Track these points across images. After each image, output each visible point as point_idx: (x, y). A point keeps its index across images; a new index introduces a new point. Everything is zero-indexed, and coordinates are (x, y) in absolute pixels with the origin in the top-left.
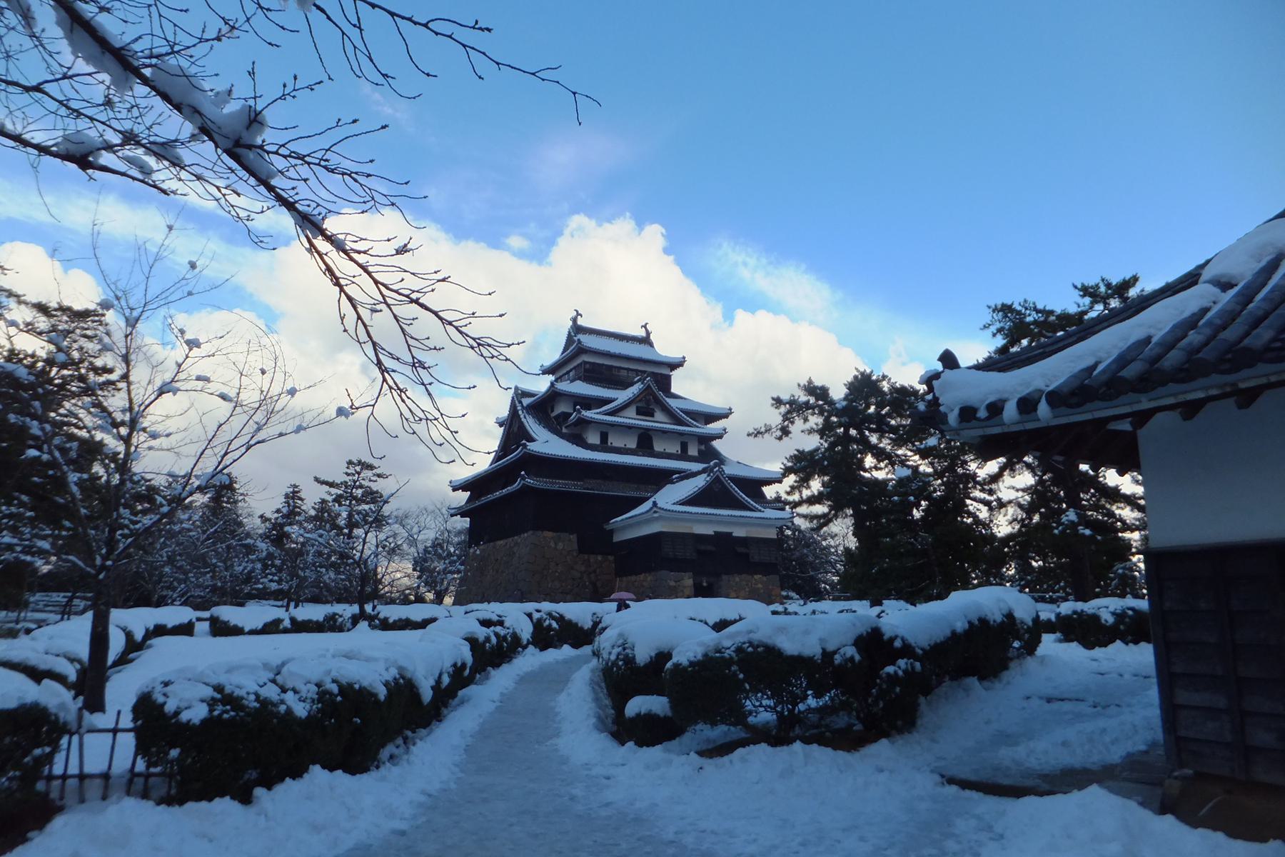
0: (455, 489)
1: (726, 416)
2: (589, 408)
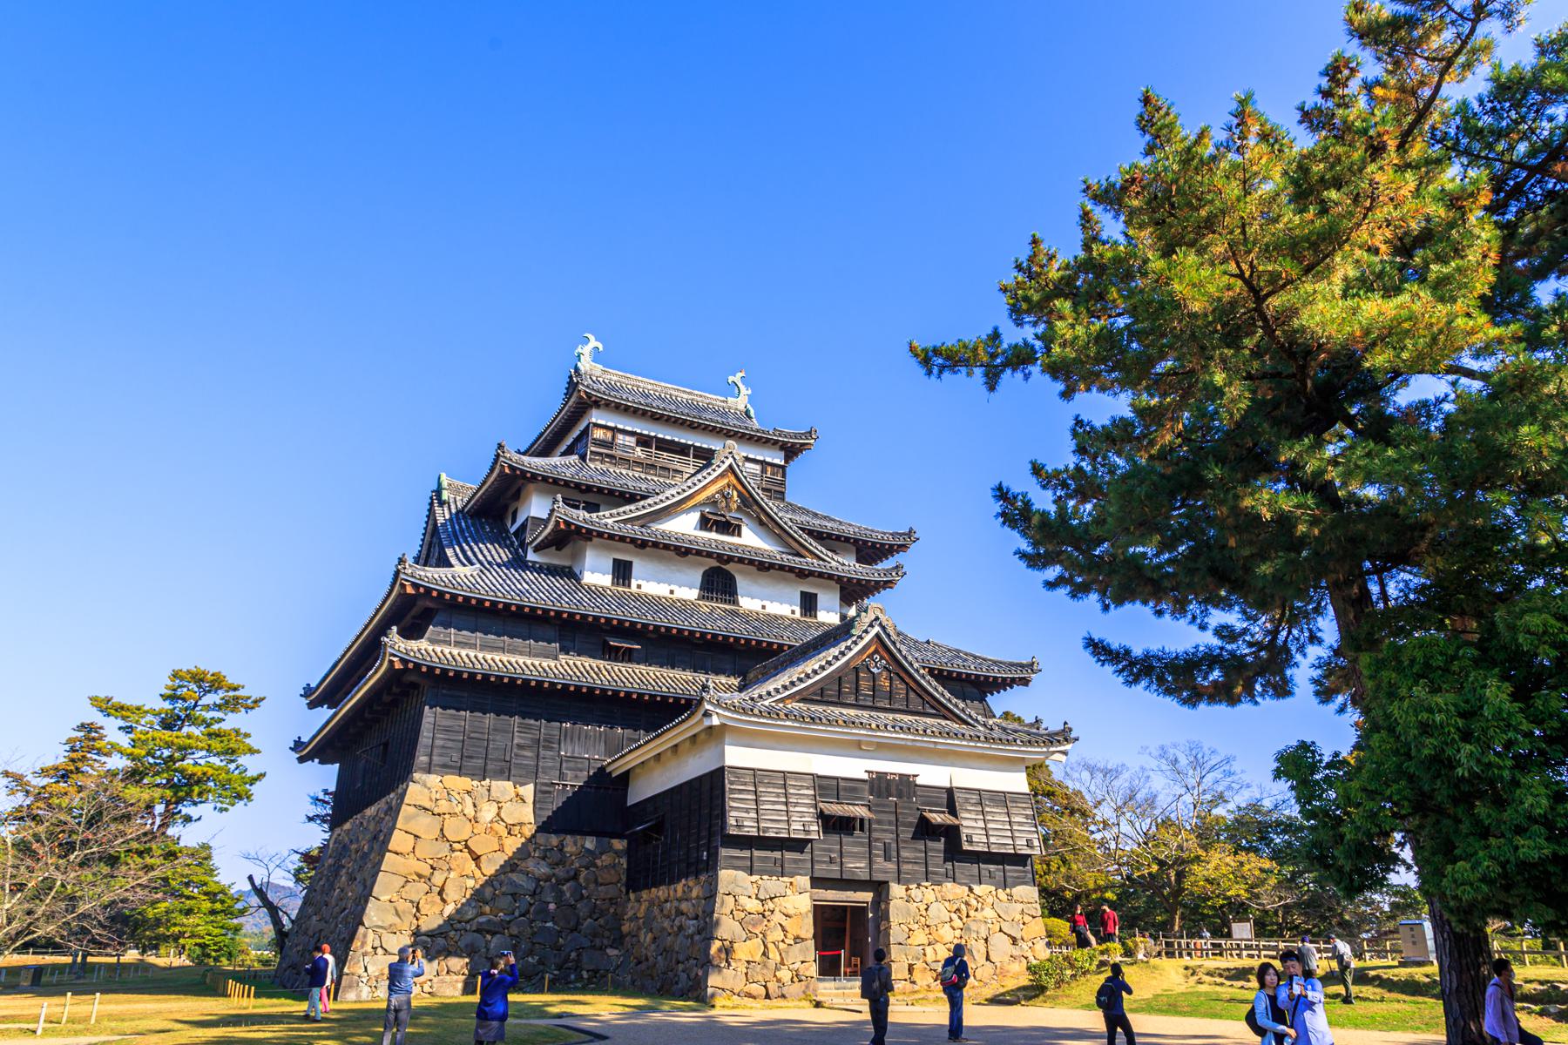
0: (312, 705)
1: (903, 548)
2: (592, 507)
